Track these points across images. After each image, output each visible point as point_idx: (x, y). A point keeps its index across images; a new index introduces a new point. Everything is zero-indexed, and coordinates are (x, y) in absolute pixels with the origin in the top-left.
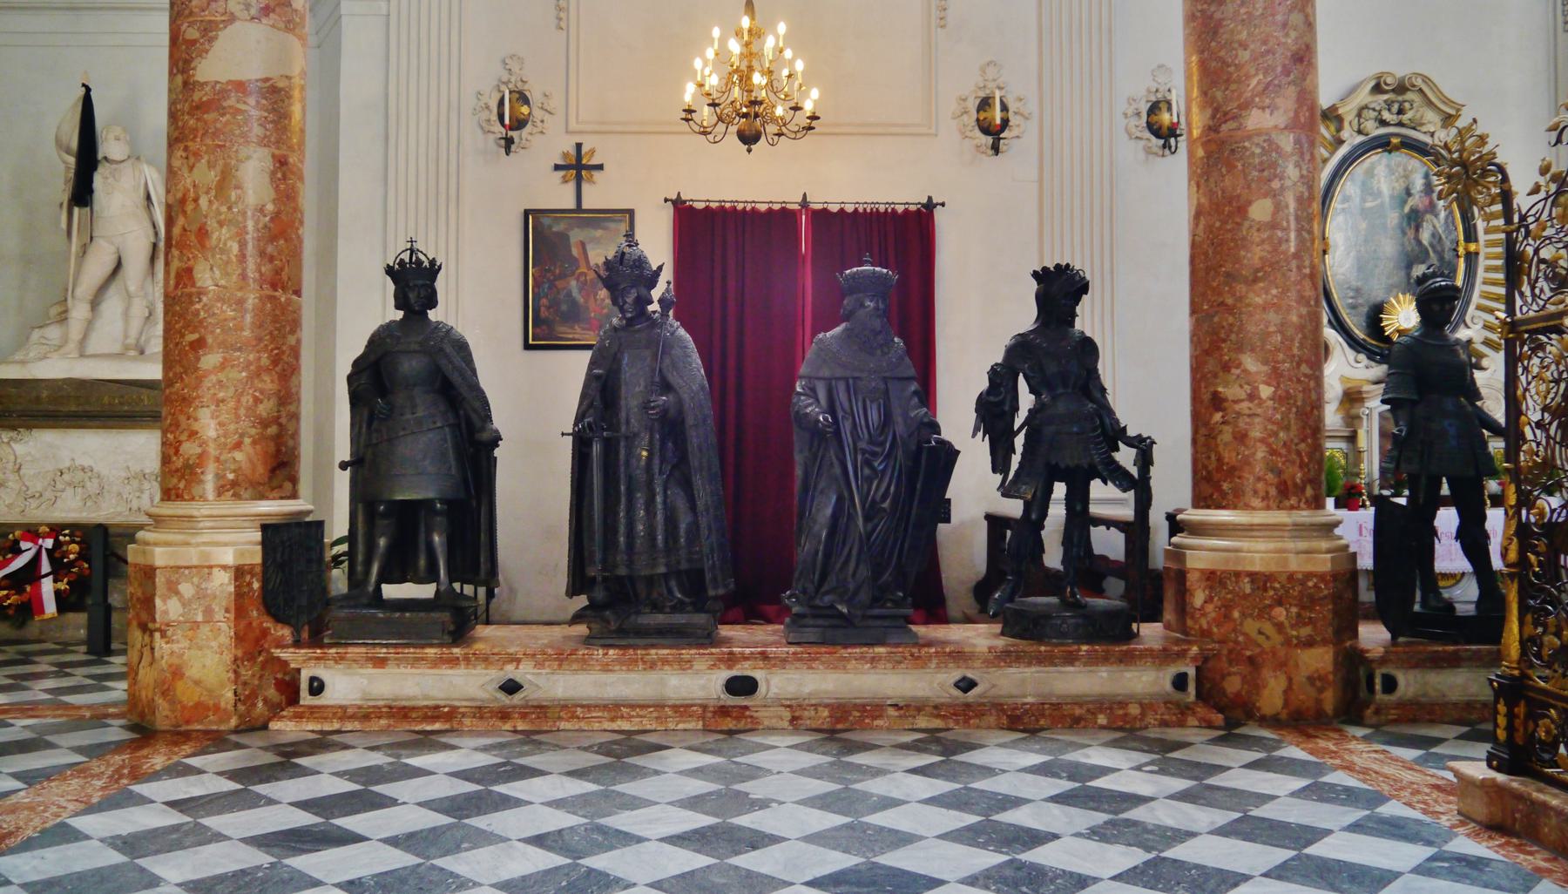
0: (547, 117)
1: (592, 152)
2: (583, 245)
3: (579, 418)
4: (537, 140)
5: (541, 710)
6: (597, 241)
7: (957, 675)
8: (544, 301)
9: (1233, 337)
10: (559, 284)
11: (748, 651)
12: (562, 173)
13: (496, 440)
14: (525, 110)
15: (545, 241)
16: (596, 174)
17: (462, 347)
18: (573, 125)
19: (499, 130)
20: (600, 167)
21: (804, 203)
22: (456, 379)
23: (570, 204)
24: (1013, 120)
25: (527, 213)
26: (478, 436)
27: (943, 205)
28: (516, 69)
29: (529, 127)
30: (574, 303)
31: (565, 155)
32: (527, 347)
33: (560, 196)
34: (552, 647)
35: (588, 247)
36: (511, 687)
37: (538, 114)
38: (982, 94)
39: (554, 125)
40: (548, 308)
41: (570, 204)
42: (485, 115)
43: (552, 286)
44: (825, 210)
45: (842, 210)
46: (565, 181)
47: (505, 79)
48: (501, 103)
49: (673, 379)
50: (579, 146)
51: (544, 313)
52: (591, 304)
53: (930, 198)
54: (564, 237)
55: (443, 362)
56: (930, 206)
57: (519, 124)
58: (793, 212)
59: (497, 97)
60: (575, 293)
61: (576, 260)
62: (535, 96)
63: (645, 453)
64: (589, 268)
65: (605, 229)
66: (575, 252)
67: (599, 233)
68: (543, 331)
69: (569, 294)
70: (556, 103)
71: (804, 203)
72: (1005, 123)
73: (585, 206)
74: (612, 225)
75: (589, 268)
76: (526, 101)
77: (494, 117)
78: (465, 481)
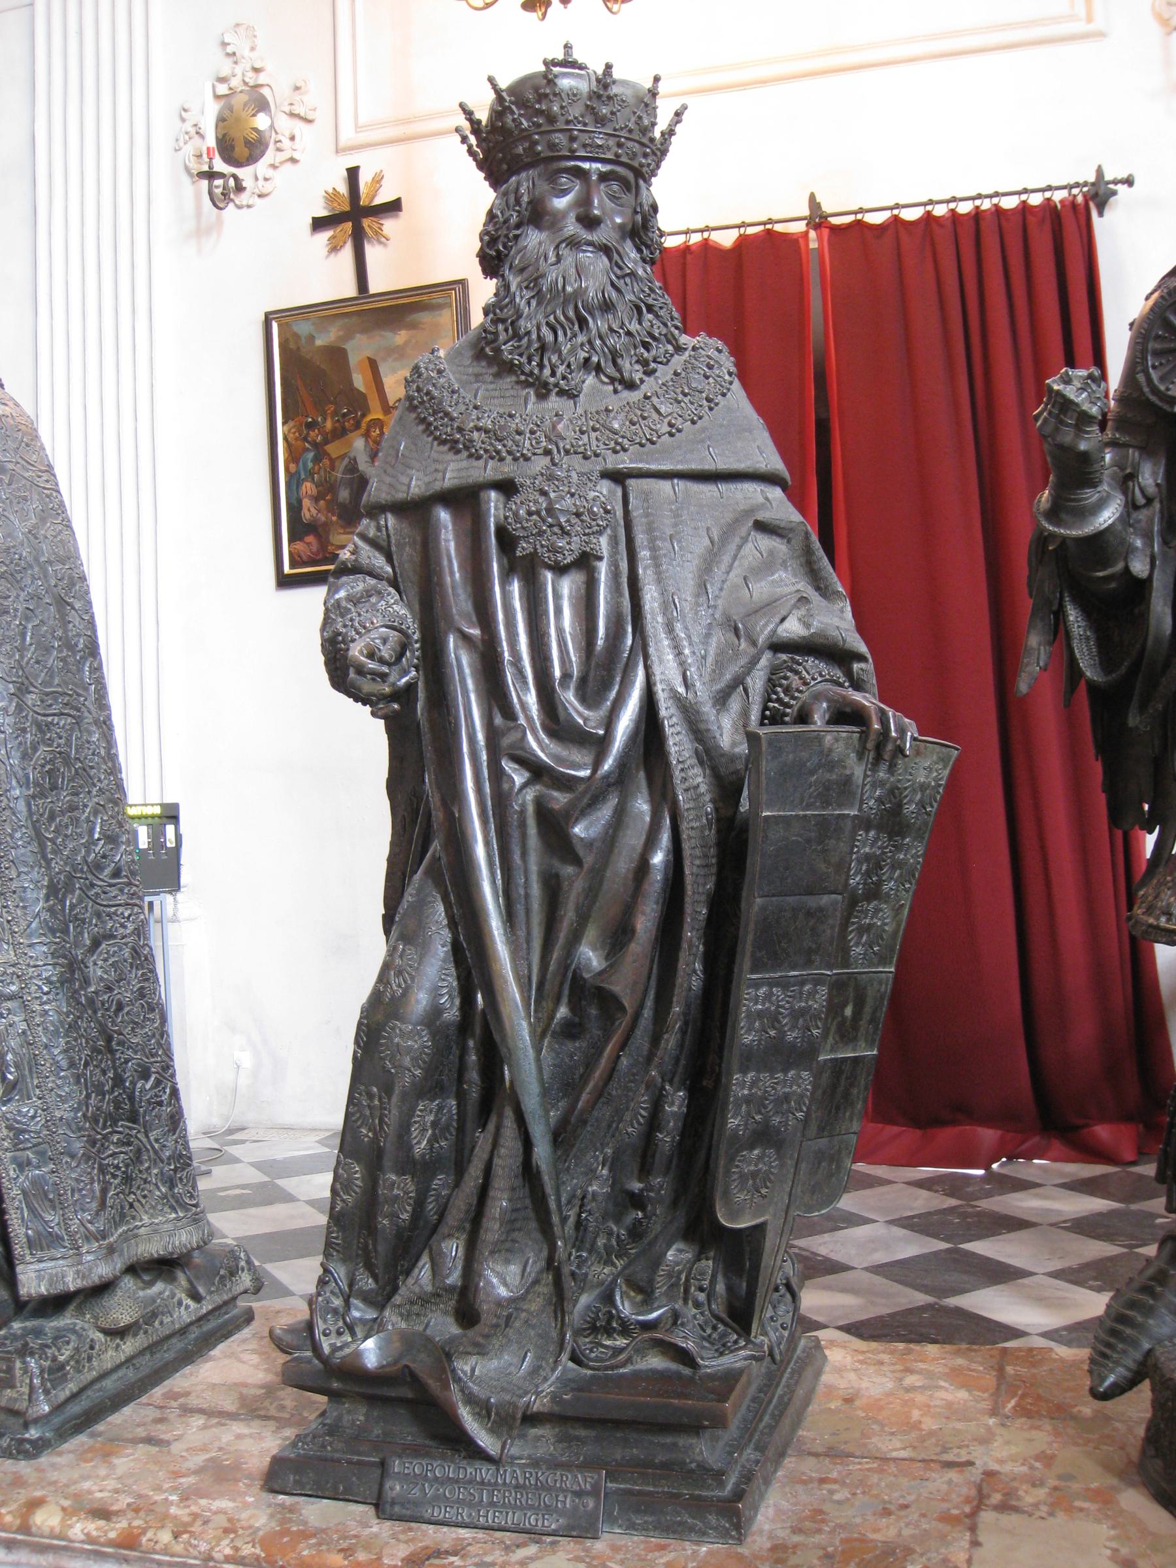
0: (298, 127)
1: (378, 180)
2: (373, 364)
10: (333, 449)
16: (389, 225)
18: (348, 135)
21: (817, 219)
27: (1129, 182)
28: (243, 50)
29: (270, 156)
32: (284, 582)
33: (324, 276)
35: (382, 369)
37: (285, 125)
39: (310, 142)
40: (316, 499)
43: (320, 451)
44: (859, 223)
45: (896, 218)
47: (225, 72)
51: (309, 511)
53: (1100, 172)
54: (337, 355)
56: (1099, 194)
58: (791, 243)
60: (363, 465)
61: (363, 397)
62: (277, 91)
64: (387, 409)
65: (413, 326)
66: (359, 381)
67: (401, 337)
69: (353, 468)
70: (315, 99)
71: (817, 219)
73: (374, 287)
74: (425, 317)
75: (387, 409)
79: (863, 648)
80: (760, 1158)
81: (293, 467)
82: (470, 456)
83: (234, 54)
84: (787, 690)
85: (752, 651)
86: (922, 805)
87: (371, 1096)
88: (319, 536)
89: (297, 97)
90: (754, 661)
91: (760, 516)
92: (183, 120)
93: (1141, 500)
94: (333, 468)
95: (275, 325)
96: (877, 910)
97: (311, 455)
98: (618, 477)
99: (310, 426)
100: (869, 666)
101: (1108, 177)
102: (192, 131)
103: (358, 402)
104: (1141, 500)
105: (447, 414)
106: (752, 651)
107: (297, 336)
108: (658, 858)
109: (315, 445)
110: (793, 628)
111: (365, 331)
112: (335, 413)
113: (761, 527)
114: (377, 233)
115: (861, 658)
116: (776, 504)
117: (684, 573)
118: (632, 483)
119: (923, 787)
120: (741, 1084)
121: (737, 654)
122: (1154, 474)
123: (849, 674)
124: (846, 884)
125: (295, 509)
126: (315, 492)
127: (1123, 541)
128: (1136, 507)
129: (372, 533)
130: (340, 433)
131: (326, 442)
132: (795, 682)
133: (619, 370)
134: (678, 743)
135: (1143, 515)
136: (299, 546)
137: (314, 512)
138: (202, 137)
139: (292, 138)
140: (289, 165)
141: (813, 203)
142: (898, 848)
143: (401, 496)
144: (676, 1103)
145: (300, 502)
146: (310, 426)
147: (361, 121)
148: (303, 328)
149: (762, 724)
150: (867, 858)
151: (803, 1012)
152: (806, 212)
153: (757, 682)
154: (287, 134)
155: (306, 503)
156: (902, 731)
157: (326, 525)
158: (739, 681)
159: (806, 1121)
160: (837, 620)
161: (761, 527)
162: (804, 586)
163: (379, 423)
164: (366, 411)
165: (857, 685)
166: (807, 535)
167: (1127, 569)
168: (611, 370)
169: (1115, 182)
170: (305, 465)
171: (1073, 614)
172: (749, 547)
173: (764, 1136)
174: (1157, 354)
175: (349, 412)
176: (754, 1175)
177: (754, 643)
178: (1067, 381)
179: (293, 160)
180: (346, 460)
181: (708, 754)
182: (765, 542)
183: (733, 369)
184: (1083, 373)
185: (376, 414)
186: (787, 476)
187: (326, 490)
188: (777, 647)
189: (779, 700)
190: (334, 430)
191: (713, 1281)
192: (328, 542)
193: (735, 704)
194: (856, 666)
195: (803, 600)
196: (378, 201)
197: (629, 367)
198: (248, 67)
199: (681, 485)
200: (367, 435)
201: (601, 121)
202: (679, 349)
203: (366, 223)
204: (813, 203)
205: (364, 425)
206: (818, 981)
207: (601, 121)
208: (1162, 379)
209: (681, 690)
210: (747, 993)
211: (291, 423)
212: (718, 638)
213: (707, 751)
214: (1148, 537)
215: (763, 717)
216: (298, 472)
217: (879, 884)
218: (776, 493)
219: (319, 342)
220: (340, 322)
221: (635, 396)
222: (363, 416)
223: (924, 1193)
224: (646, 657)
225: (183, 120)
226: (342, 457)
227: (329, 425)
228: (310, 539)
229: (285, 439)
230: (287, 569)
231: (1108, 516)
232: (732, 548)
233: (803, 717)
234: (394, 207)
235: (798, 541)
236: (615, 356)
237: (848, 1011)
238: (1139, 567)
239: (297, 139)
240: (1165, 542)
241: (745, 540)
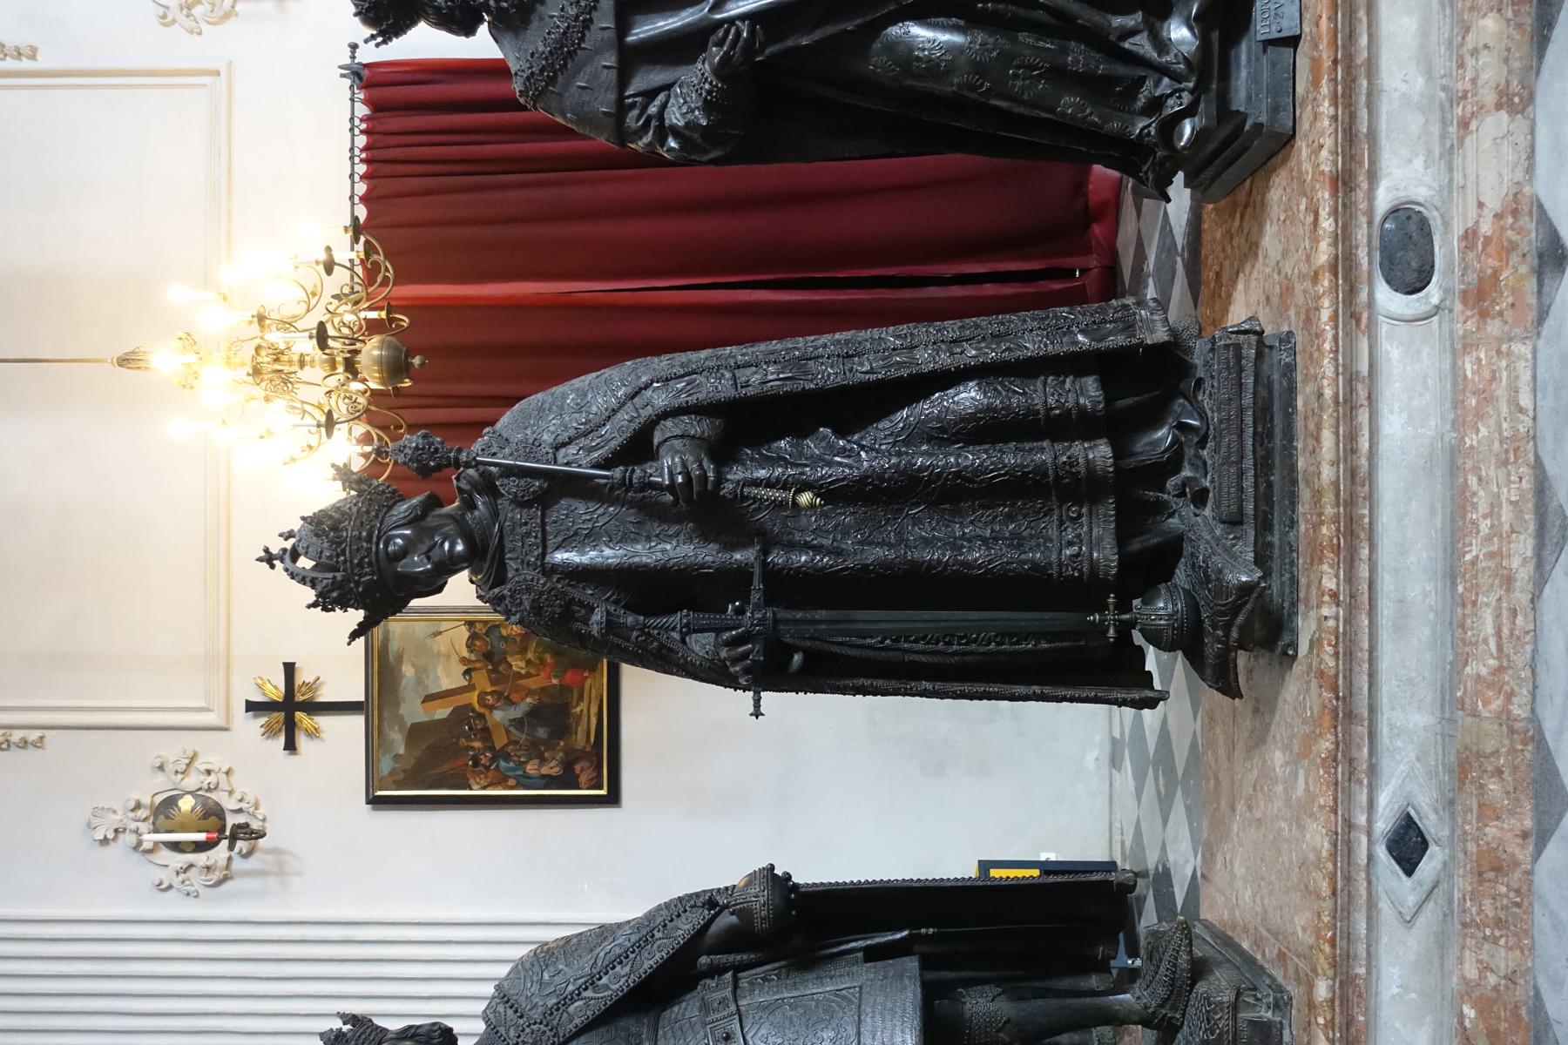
0: (200, 765)
2: (429, 698)
3: (715, 673)
4: (241, 784)
5: (1464, 768)
6: (422, 672)
8: (531, 768)
11: (1327, 224)
12: (302, 740)
13: (774, 881)
14: (186, 804)
15: (430, 764)
16: (303, 677)
17: (545, 956)
19: (221, 852)
20: (289, 669)
22: (616, 983)
23: (355, 725)
25: (376, 802)
26: (760, 925)
27: (354, 47)
28: (115, 820)
30: (534, 714)
31: (270, 732)
32: (613, 799)
33: (340, 744)
34: (1310, 740)
36: (1408, 845)
37: (192, 782)
39: (214, 754)
40: (543, 760)
41: (355, 725)
42: (196, 879)
46: (313, 734)
48: (176, 847)
49: (614, 434)
50: (251, 707)
51: (552, 768)
52: (533, 684)
54: (416, 733)
55: (578, 1012)
57: (212, 815)
59: (166, 856)
60: (517, 712)
63: (805, 498)
64: (470, 688)
65: (400, 658)
66: (442, 712)
67: (408, 671)
68: (581, 766)
69: (518, 723)
70: (172, 749)
74: (394, 646)
75: (470, 688)
76: (171, 802)
77: (201, 858)
78: (873, 954)
81: (512, 782)
82: (595, 8)
83: (116, 831)
87: (1016, 76)
88: (576, 760)
89: (170, 767)
92: (170, 887)
94: (517, 742)
95: (379, 793)
97: (502, 763)
99: (476, 763)
101: (349, 61)
102: (182, 876)
103: (461, 714)
105: (565, 33)
107: (392, 773)
109: (494, 759)
111: (398, 705)
112: (468, 738)
114: (310, 689)
125: (550, 782)
126: (536, 761)
129: (635, 112)
130: (486, 733)
131: (492, 748)
136: (583, 779)
137: (554, 763)
138: (191, 866)
139: (209, 772)
140: (232, 779)
143: (613, 74)
145: (543, 776)
146: (476, 763)
147: (203, 704)
148: (386, 765)
154: (202, 777)
155: (545, 770)
157: (568, 751)
163: (482, 695)
164: (469, 707)
169: (353, 57)
170: (513, 770)
175: (469, 724)
179: (227, 773)
180: (512, 729)
185: (473, 698)
187: (536, 750)
190: (483, 740)
192: (583, 751)
196: (282, 689)
198: (132, 815)
200: (491, 708)
203: (299, 698)
205: (481, 710)
211: (472, 781)
216: (516, 777)
219: (401, 751)
220: (386, 729)
222: (473, 710)
225: (170, 887)
226: (508, 731)
227: (477, 744)
228: (577, 768)
229: (484, 788)
230: (603, 792)
234: (289, 669)
239: (209, 767)
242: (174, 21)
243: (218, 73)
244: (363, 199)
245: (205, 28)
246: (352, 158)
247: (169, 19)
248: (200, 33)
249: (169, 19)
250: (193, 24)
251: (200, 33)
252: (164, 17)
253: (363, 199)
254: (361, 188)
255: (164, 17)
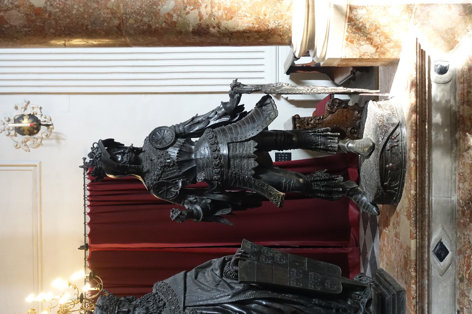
7: (434, 259)
9: (145, 19)
21: (85, 247)
24: (29, 111)
38: (13, 133)
45: (89, 224)
71: (85, 247)
72: (32, 116)
79: (223, 258)
80: (327, 284)
84: (231, 274)
85: (222, 281)
86: (255, 247)
90: (225, 281)
91: (194, 278)
93: (195, 200)
96: (277, 258)
98: (185, 308)
100: (226, 257)
104: (195, 200)
106: (222, 281)
108: (264, 303)
110: (218, 272)
113: (196, 278)
115: (225, 258)
116: (191, 274)
117: (205, 295)
118: (186, 305)
119: (252, 247)
120: (311, 287)
121: (223, 284)
122: (190, 197)
123: (227, 261)
124: (271, 264)
127: (204, 204)
128: (197, 201)
132: (229, 273)
133: (161, 306)
134: (241, 298)
135: (198, 200)
141: (81, 248)
142: (264, 252)
144: (316, 301)
149: (237, 280)
150: (265, 260)
151: (297, 274)
152: (83, 251)
153: (229, 281)
156: (240, 252)
158: (228, 284)
159: (320, 274)
160: (217, 262)
161: (196, 278)
162: (209, 269)
165: (230, 259)
166: (198, 268)
167: (209, 204)
168: (161, 308)
171: (217, 214)
172: (201, 281)
173: (322, 283)
174: (166, 196)
176: (331, 285)
177: (221, 281)
178: (173, 216)
181: (243, 291)
182: (199, 277)
183: (161, 282)
184: (171, 213)
186: (184, 271)
188: (221, 276)
189: (233, 276)
191: (357, 294)
193: (233, 285)
194: (226, 260)
195: (212, 270)
197: (161, 304)
199: (187, 294)
201: (107, 308)
202: (157, 293)
204: (81, 248)
206: (290, 271)
207: (107, 308)
208: (172, 195)
209: (230, 296)
210: (292, 285)
212: (219, 288)
213: (243, 292)
214: (203, 199)
215: (236, 280)
217: (271, 257)
218: (188, 274)
221: (167, 303)
223: (367, 231)
224: (223, 303)
231: (198, 208)
232: (201, 285)
233: (236, 271)
235: (199, 270)
236: (158, 307)
237: (297, 264)
238: (209, 201)
240: (204, 196)
241: (199, 281)
242: (20, 147)
243: (36, 166)
244: (88, 214)
245: (31, 149)
246: (84, 199)
247: (18, 147)
248: (29, 151)
249: (18, 147)
250: (27, 148)
251: (29, 151)
252: (17, 146)
253: (88, 214)
254: (88, 210)
255: (17, 146)
